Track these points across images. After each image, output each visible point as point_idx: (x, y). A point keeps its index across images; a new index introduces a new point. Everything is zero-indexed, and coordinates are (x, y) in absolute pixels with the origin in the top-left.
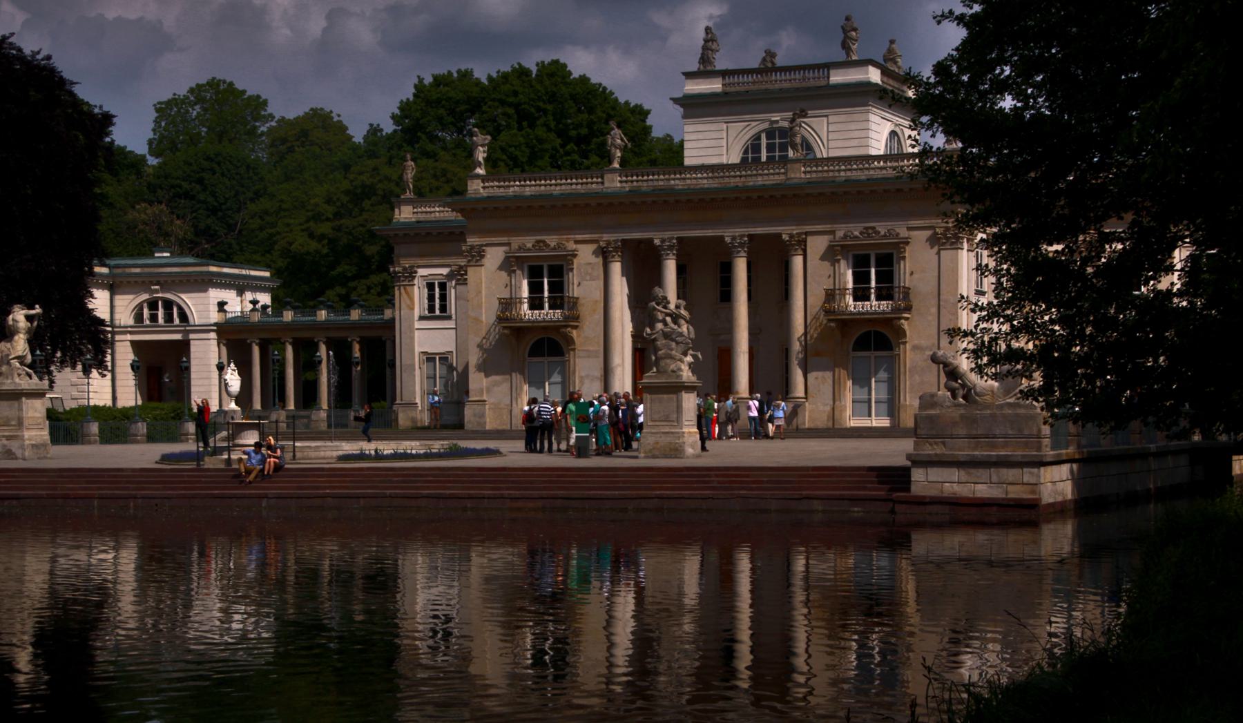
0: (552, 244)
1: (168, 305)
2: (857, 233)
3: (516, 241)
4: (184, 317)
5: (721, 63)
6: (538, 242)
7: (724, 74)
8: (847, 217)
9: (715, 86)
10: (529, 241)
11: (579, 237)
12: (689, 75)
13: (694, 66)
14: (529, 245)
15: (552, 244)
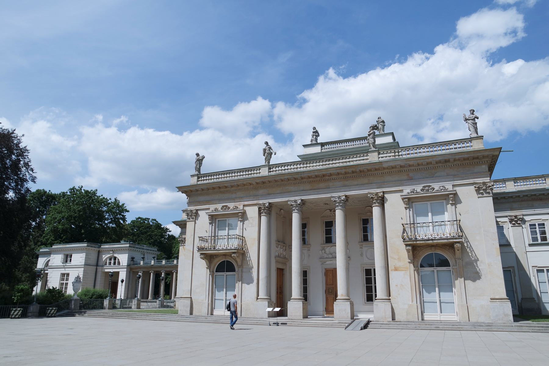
0: (231, 208)
1: (115, 258)
2: (419, 190)
3: (212, 207)
4: (119, 263)
5: (319, 141)
6: (223, 207)
7: (322, 145)
8: (411, 180)
9: (317, 149)
10: (219, 206)
11: (246, 203)
12: (305, 146)
13: (310, 143)
14: (220, 209)
15: (231, 208)
